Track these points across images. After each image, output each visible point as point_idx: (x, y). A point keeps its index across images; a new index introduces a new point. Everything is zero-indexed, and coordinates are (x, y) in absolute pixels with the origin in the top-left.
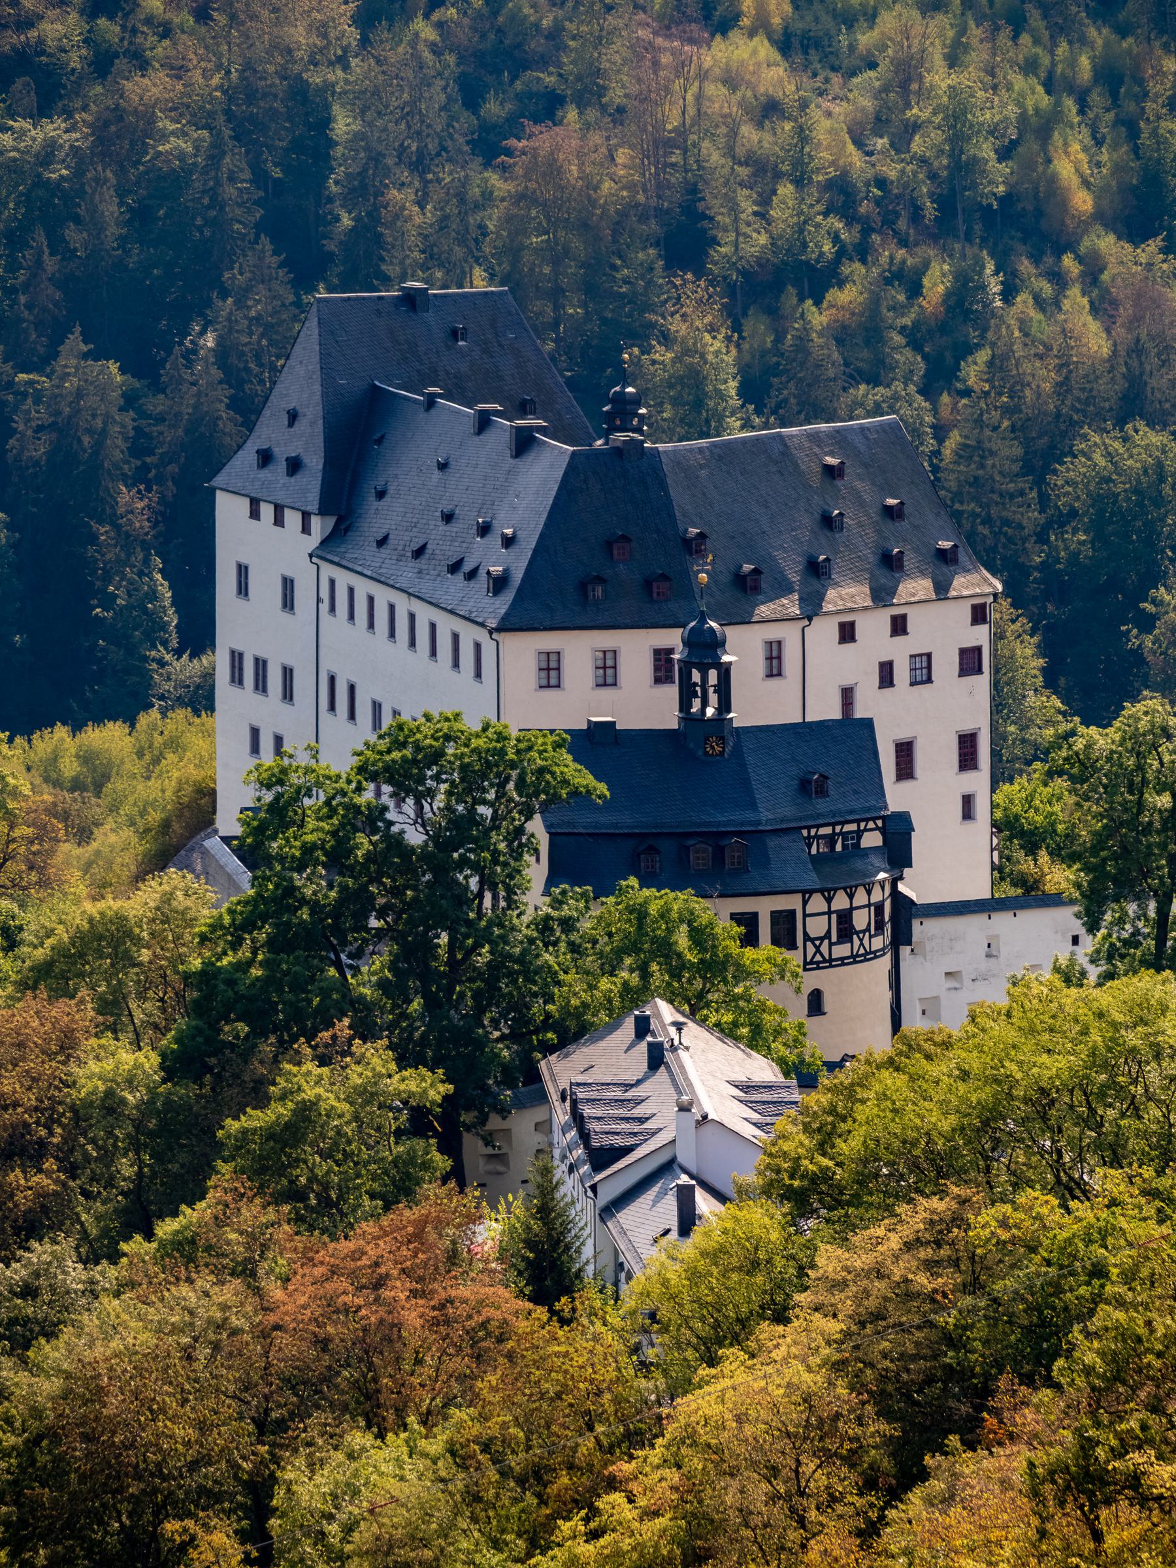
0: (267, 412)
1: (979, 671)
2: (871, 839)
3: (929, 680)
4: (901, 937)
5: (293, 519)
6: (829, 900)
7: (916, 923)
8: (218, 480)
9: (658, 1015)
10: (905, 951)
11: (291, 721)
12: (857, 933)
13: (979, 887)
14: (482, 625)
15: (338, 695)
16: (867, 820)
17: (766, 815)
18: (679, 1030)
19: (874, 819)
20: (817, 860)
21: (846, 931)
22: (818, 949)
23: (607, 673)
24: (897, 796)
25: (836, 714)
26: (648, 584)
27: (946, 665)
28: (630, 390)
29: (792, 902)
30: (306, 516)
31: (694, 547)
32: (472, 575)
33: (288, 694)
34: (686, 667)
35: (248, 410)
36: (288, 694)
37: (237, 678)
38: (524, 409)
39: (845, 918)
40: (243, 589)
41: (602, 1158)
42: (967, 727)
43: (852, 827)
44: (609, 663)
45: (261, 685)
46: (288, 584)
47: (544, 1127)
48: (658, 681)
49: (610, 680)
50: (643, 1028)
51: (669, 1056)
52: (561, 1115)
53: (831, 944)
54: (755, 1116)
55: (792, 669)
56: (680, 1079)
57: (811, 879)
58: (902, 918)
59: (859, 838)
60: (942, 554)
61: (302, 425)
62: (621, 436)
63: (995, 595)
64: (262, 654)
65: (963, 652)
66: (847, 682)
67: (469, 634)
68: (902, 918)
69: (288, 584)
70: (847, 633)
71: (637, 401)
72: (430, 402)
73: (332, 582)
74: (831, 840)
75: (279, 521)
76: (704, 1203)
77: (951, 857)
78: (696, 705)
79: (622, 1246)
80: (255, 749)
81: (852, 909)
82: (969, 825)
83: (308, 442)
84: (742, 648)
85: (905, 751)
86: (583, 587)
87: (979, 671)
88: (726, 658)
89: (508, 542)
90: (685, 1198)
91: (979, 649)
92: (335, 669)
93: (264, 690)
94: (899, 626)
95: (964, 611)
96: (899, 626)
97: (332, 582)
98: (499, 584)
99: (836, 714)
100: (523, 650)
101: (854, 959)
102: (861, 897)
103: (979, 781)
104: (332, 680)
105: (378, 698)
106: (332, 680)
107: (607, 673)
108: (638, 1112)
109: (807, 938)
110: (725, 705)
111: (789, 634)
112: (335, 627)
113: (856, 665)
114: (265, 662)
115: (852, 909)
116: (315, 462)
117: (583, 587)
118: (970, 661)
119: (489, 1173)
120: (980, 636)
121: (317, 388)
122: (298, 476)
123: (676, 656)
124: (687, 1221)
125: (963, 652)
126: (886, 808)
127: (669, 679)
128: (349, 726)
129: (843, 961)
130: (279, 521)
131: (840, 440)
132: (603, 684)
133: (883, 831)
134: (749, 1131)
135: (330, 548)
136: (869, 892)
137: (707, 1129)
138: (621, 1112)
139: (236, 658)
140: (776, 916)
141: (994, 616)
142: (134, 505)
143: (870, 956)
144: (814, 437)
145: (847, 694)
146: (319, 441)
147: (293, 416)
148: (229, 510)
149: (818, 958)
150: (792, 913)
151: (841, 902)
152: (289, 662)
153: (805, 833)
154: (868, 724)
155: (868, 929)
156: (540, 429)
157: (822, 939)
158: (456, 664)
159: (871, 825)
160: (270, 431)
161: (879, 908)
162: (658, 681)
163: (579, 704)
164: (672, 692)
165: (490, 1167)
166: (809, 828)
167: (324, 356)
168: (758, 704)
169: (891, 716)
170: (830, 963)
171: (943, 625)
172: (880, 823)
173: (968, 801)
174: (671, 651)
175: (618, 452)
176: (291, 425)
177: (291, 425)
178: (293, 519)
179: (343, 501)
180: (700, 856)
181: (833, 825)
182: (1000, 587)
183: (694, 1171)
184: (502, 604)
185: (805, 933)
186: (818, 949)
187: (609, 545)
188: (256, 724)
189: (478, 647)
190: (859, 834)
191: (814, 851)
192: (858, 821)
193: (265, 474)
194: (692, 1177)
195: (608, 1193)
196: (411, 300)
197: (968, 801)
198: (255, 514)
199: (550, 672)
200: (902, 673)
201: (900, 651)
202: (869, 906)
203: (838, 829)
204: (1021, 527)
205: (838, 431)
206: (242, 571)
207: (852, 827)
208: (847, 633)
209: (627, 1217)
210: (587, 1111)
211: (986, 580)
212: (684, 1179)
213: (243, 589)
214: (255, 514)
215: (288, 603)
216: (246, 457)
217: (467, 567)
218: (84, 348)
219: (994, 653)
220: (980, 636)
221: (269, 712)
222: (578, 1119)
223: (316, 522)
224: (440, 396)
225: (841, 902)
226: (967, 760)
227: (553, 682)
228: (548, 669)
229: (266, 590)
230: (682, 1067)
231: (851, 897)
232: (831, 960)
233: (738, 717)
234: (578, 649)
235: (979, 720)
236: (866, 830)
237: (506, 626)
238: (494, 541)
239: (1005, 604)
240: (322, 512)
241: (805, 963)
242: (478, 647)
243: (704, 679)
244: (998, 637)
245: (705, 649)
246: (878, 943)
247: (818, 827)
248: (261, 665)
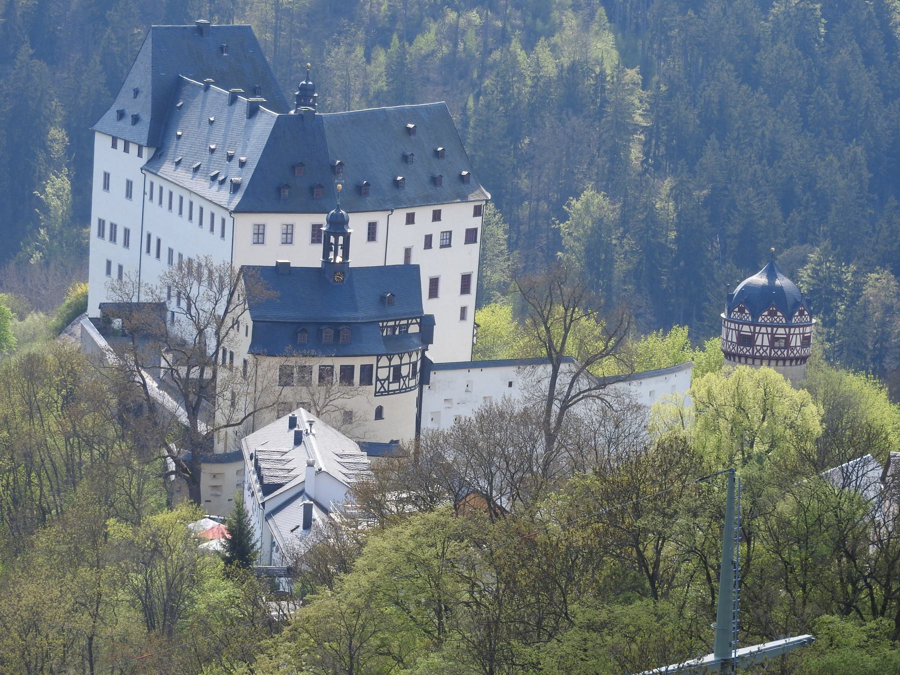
0: (123, 90)
1: (475, 242)
2: (414, 329)
3: (449, 245)
4: (424, 380)
5: (134, 149)
6: (390, 360)
7: (432, 373)
8: (97, 126)
9: (301, 417)
10: (426, 387)
11: (127, 257)
12: (403, 377)
13: (465, 356)
14: (227, 209)
16: (412, 319)
17: (361, 315)
18: (311, 425)
19: (416, 318)
20: (386, 339)
21: (397, 376)
22: (382, 385)
23: (288, 237)
24: (429, 306)
25: (402, 263)
26: (312, 189)
27: (459, 238)
28: (310, 83)
29: (371, 360)
30: (140, 147)
31: (334, 170)
32: (222, 182)
33: (126, 243)
34: (328, 234)
35: (115, 86)
36: (126, 243)
37: (101, 234)
38: (254, 92)
39: (397, 369)
40: (106, 186)
41: (268, 489)
42: (466, 271)
43: (405, 322)
44: (289, 231)
45: (113, 238)
46: (129, 184)
47: (241, 472)
48: (313, 242)
49: (289, 241)
50: (293, 423)
51: (304, 438)
52: (250, 466)
53: (389, 383)
54: (345, 471)
55: (379, 240)
56: (309, 450)
57: (382, 349)
59: (408, 328)
60: (462, 177)
61: (141, 97)
62: (303, 108)
63: (487, 201)
64: (115, 222)
65: (468, 231)
66: (408, 246)
67: (219, 214)
68: (426, 370)
69: (129, 184)
70: (410, 219)
71: (313, 89)
72: (207, 88)
73: (152, 184)
74: (394, 328)
75: (126, 150)
76: (316, 514)
77: (451, 341)
78: (331, 256)
79: (275, 533)
80: (108, 272)
81: (401, 365)
82: (463, 322)
83: (143, 107)
84: (357, 224)
85: (434, 283)
86: (278, 190)
87: (475, 242)
88: (349, 231)
89: (242, 164)
90: (308, 510)
91: (476, 230)
92: (150, 231)
93: (115, 241)
94: (437, 216)
95: (469, 208)
96: (437, 216)
97: (152, 184)
98: (235, 187)
99: (401, 262)
100: (247, 222)
101: (400, 391)
102: (406, 359)
103: (470, 300)
104: (149, 236)
105: (172, 247)
106: (149, 236)
107: (288, 237)
108: (288, 466)
109: (377, 379)
110: (346, 255)
111: (379, 217)
112: (152, 207)
113: (413, 236)
114: (116, 226)
115: (401, 365)
116: (146, 118)
117: (278, 190)
119: (212, 495)
120: (477, 223)
121: (150, 77)
122: (137, 125)
123: (324, 229)
124: (308, 523)
125: (468, 231)
126: (422, 312)
127: (319, 241)
128: (156, 261)
129: (394, 392)
130: (126, 150)
131: (413, 115)
132: (285, 242)
133: (420, 325)
134: (341, 478)
136: (410, 356)
137: (321, 475)
138: (280, 466)
139: (101, 223)
140: (363, 368)
141: (486, 211)
142: (57, 135)
143: (408, 389)
144: (402, 112)
145: (408, 252)
146: (149, 106)
147: (136, 92)
148: (101, 143)
149: (382, 390)
150: (372, 366)
151: (396, 361)
152: (128, 227)
153: (381, 324)
154: (417, 268)
155: (408, 376)
156: (262, 103)
157: (385, 380)
158: (212, 230)
159: (414, 321)
160: (124, 101)
161: (415, 364)
162: (313, 242)
163: (269, 255)
164: (320, 248)
165: (214, 492)
166: (383, 322)
167: (154, 59)
168: (363, 255)
169: (429, 264)
170: (388, 392)
171: (459, 216)
172: (418, 320)
173: (463, 310)
174: (321, 226)
175: (301, 117)
176: (135, 97)
177: (135, 97)
178: (134, 149)
179: (158, 144)
180: (328, 334)
181: (395, 320)
182: (489, 197)
183: (313, 496)
184: (237, 199)
185: (377, 377)
186: (382, 385)
187: (293, 167)
188: (110, 259)
189: (223, 221)
190: (408, 325)
191: (384, 334)
192: (408, 319)
193: (121, 124)
194: (311, 499)
195: (269, 507)
196: (200, 29)
197: (463, 310)
198: (114, 146)
199: (259, 235)
200: (436, 242)
201: (435, 230)
202: (409, 364)
203: (397, 323)
204: (504, 166)
205: (414, 109)
206: (107, 176)
207: (405, 322)
208: (410, 219)
209: (278, 517)
210: (263, 465)
211: (483, 193)
212: (307, 501)
213: (106, 186)
214: (114, 146)
215: (129, 194)
216: (112, 114)
217: (221, 178)
218: (31, 51)
219: (483, 232)
220: (477, 223)
221: (116, 252)
222: (258, 469)
223: (145, 151)
224: (212, 83)
225: (396, 361)
226: (465, 288)
227: (260, 241)
228: (258, 234)
229: (118, 187)
230: (311, 444)
231: (401, 359)
232: (389, 391)
233: (354, 262)
235: (472, 268)
236: (412, 324)
237: (239, 210)
238: (235, 164)
239: (491, 205)
240: (149, 145)
241: (376, 392)
242: (223, 221)
243: (337, 240)
244: (486, 224)
245: (338, 226)
246: (412, 383)
247: (388, 321)
248: (113, 227)
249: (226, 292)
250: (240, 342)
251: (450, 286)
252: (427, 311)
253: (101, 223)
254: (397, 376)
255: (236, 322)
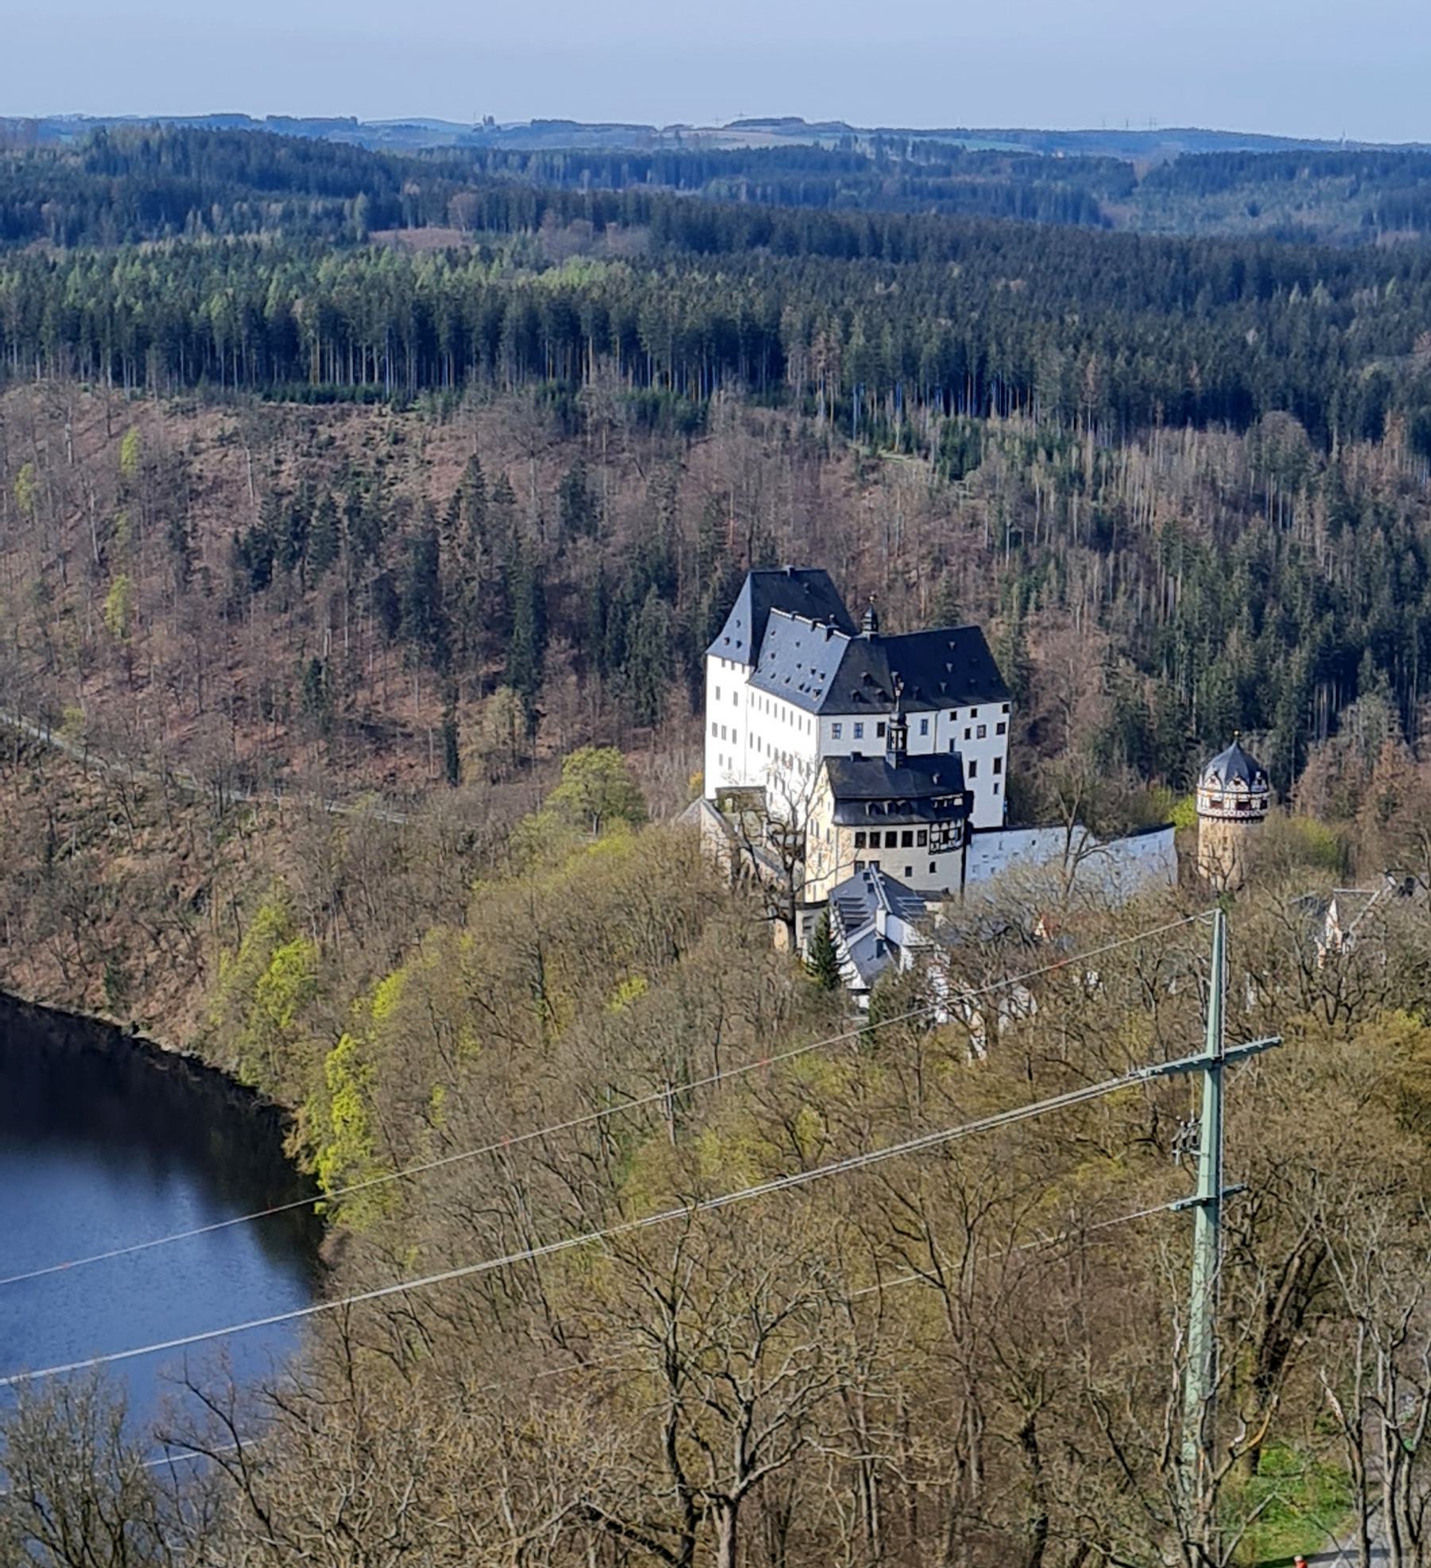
2: (958, 802)
4: (967, 841)
15: (755, 742)
20: (936, 811)
21: (946, 839)
23: (859, 731)
27: (992, 729)
29: (926, 827)
37: (715, 734)
39: (946, 833)
58: (969, 831)
68: (969, 831)
70: (954, 716)
84: (913, 720)
85: (973, 765)
94: (974, 714)
95: (999, 706)
96: (974, 714)
99: (947, 750)
101: (948, 850)
103: (1001, 778)
107: (859, 731)
111: (930, 716)
112: (754, 711)
118: (1001, 729)
120: (1005, 718)
135: (751, 681)
139: (715, 726)
145: (952, 742)
148: (713, 664)
151: (945, 827)
164: (884, 740)
168: (917, 746)
169: (968, 752)
170: (939, 851)
199: (837, 730)
200: (973, 734)
208: (954, 716)
215: (735, 702)
225: (945, 827)
226: (997, 770)
229: (727, 696)
234: (848, 722)
249: (812, 777)
250: (825, 813)
251: (985, 768)
252: (968, 788)
253: (715, 726)
254: (946, 839)
255: (820, 799)
